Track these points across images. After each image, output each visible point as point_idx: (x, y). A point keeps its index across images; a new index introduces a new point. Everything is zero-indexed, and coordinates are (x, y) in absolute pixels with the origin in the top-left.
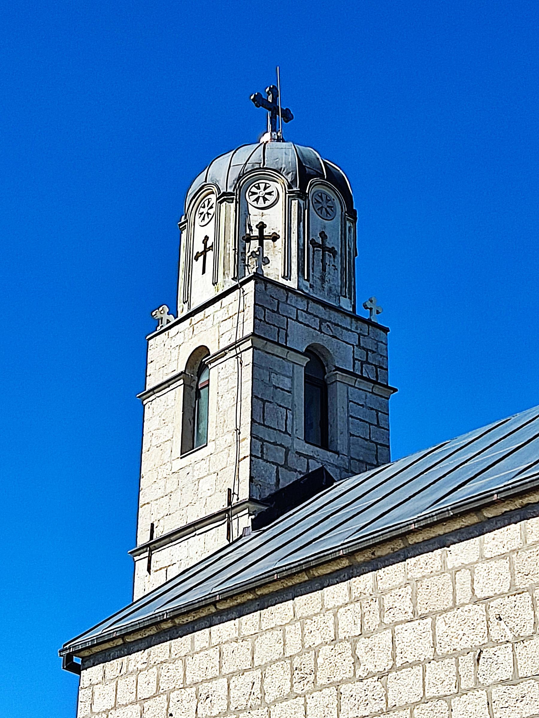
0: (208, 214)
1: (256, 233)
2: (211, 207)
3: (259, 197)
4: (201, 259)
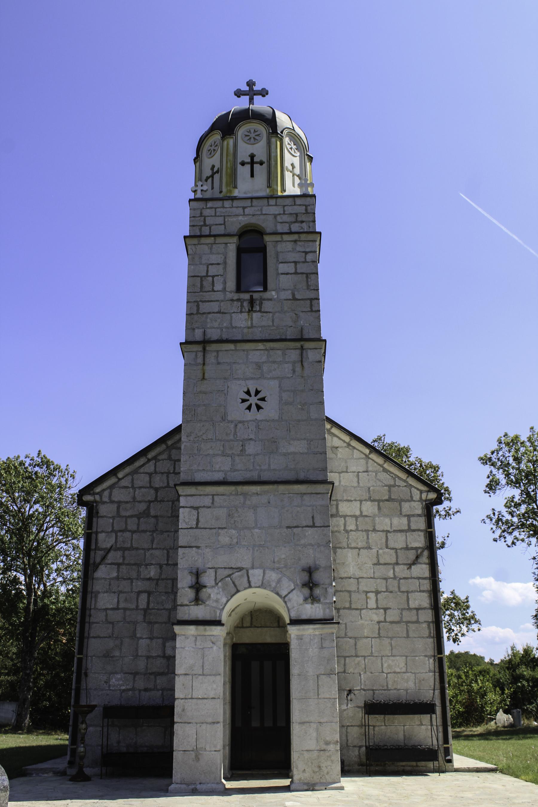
0: (214, 150)
1: (248, 160)
2: (217, 145)
3: (250, 138)
4: (210, 180)
